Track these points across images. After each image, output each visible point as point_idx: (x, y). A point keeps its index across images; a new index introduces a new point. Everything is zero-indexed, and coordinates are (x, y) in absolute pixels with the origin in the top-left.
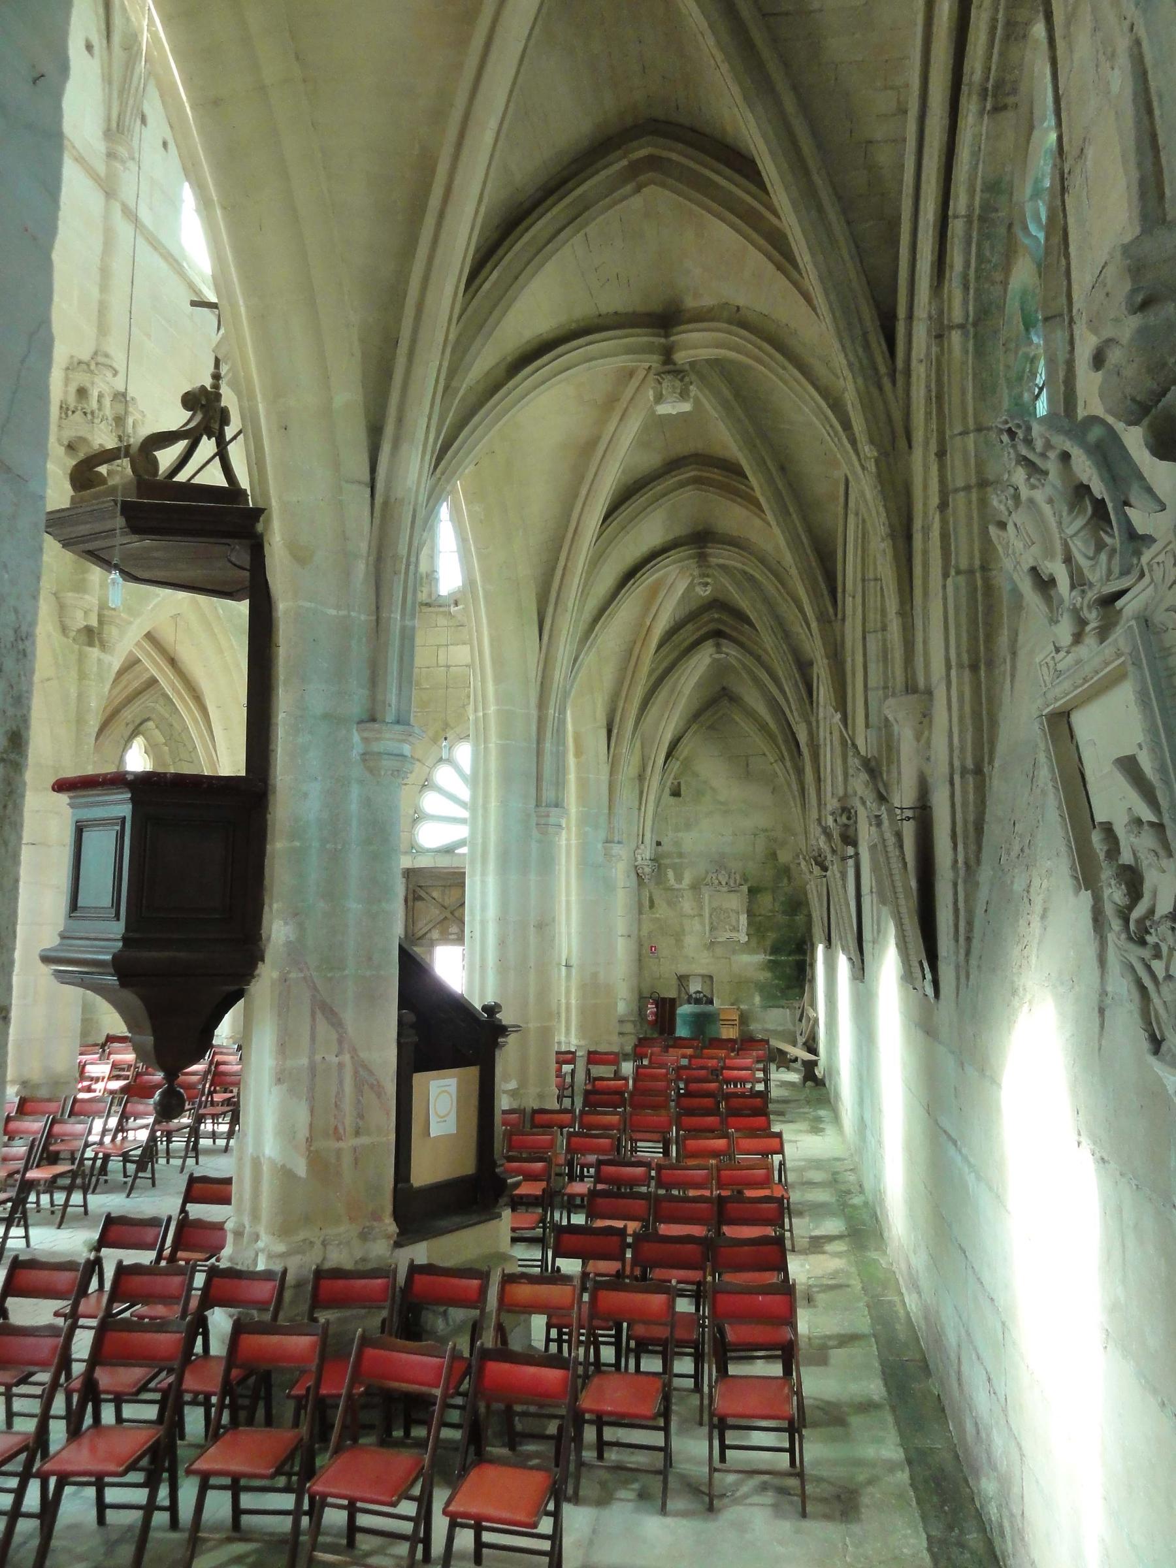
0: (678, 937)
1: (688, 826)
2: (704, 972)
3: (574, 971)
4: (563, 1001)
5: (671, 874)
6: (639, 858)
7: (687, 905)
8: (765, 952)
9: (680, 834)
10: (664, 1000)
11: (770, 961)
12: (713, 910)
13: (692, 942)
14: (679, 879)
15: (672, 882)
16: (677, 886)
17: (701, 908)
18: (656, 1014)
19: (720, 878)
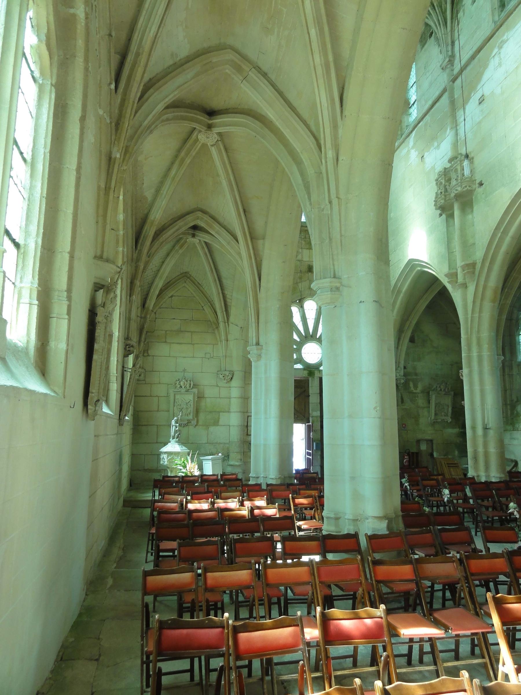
0: (416, 418)
1: (419, 359)
2: (430, 438)
3: (491, 433)
4: (481, 450)
5: (411, 385)
6: (398, 375)
7: (421, 401)
8: (459, 427)
9: (415, 363)
10: (413, 453)
11: (461, 432)
12: (436, 405)
13: (423, 421)
14: (416, 387)
15: (412, 389)
16: (415, 391)
17: (429, 402)
18: (409, 461)
19: (442, 387)
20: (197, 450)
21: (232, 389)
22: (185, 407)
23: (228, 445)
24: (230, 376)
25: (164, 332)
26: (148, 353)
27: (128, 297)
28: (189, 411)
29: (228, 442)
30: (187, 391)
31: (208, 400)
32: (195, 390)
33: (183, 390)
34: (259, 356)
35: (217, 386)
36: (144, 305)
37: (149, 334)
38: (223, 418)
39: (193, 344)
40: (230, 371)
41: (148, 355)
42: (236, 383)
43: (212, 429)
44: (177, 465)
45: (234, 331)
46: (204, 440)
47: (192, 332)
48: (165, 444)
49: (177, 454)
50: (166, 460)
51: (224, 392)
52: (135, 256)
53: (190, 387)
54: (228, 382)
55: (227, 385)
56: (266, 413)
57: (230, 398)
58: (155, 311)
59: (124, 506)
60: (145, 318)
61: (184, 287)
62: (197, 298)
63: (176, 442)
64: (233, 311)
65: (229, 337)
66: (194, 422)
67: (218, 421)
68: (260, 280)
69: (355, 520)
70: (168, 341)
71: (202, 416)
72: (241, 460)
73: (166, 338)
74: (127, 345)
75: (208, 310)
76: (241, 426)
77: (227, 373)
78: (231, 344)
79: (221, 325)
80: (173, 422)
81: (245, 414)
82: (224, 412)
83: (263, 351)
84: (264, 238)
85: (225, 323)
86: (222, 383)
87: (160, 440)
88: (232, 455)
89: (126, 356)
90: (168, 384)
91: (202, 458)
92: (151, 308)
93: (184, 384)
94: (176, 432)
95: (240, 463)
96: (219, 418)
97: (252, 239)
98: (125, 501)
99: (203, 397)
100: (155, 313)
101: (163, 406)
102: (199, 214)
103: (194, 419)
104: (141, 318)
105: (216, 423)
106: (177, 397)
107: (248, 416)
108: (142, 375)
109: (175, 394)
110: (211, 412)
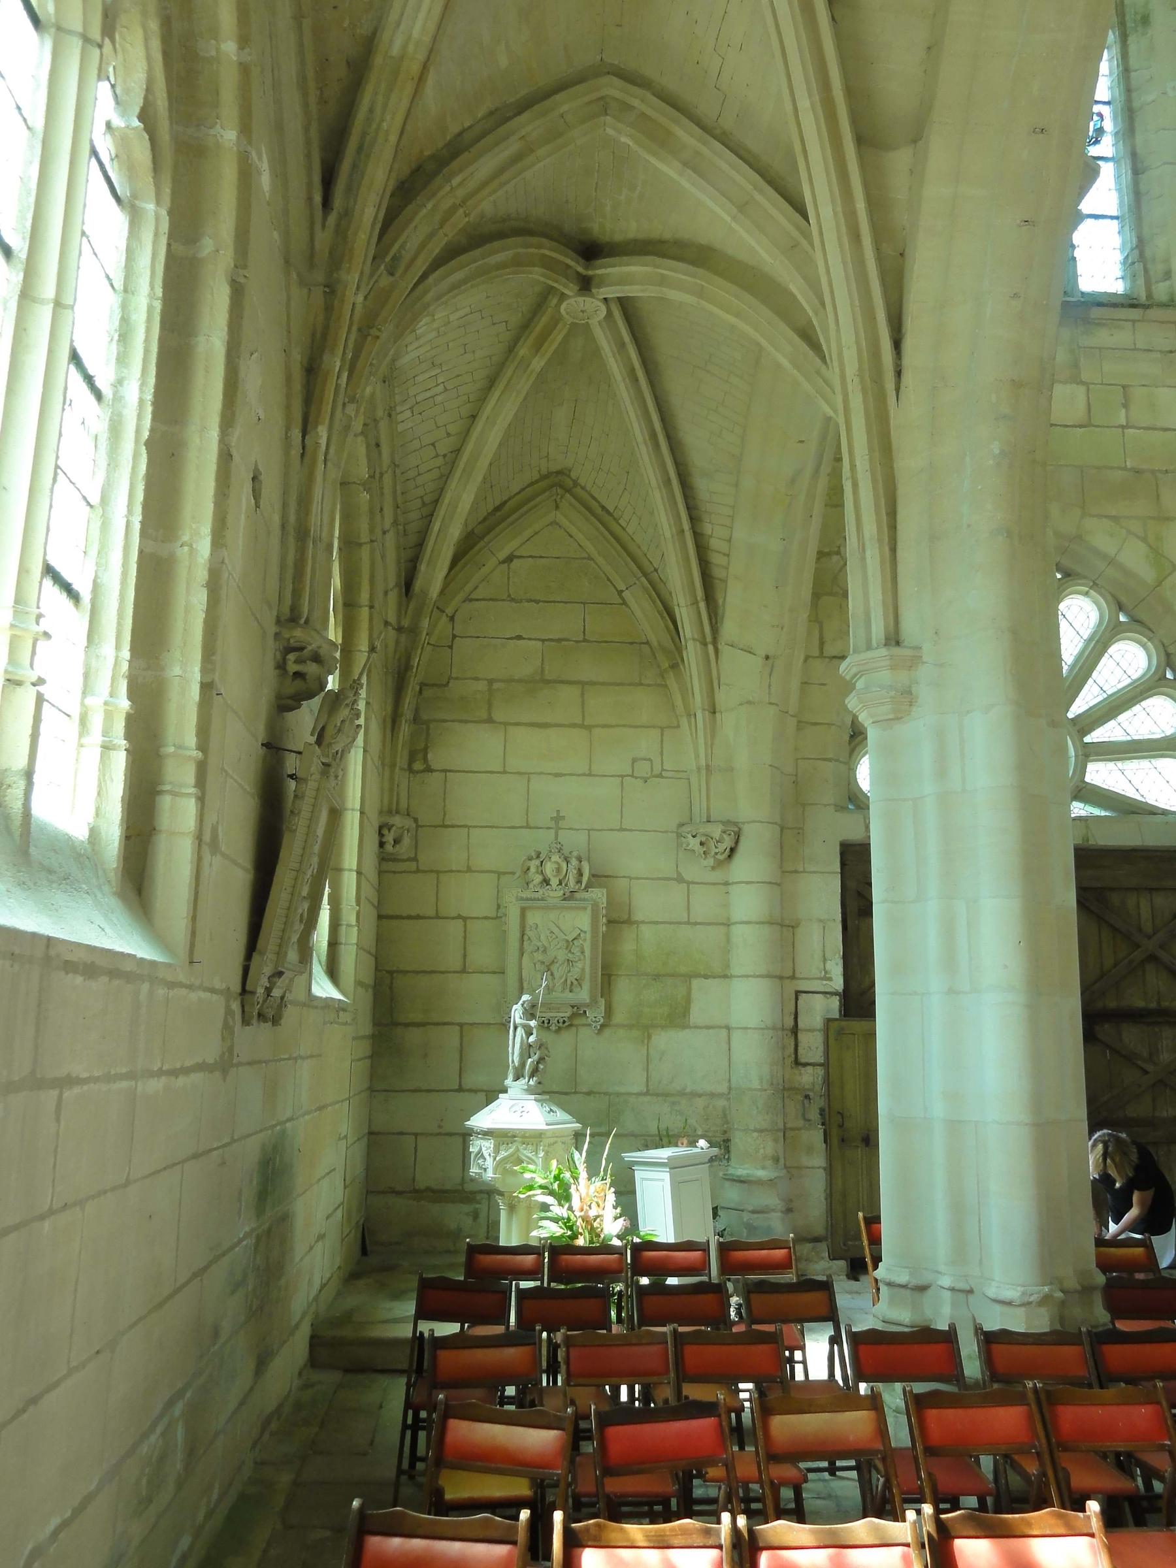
20: (609, 1125)
21: (734, 889)
22: (561, 955)
23: (721, 1103)
24: (728, 843)
25: (482, 686)
26: (425, 759)
27: (296, 433)
28: (576, 972)
29: (723, 1088)
30: (570, 896)
31: (646, 931)
32: (598, 895)
33: (554, 894)
34: (904, 700)
35: (680, 879)
36: (407, 586)
37: (428, 693)
38: (706, 1000)
39: (589, 728)
40: (728, 823)
41: (429, 770)
42: (751, 866)
43: (663, 1040)
44: (531, 1188)
45: (741, 675)
46: (635, 1083)
47: (583, 684)
48: (491, 1095)
49: (533, 1138)
50: (489, 1163)
51: (704, 904)
52: (323, 239)
53: (579, 882)
54: (718, 865)
55: (717, 876)
56: (950, 962)
57: (728, 924)
58: (449, 611)
59: (314, 1361)
60: (413, 631)
61: (554, 523)
62: (600, 560)
63: (530, 1091)
64: (733, 599)
65: (721, 696)
66: (596, 1015)
67: (686, 1012)
68: (897, 344)
70: (498, 715)
71: (625, 993)
72: (776, 1160)
73: (490, 706)
74: (289, 650)
75: (641, 607)
76: (774, 1028)
77: (716, 831)
78: (728, 722)
79: (692, 653)
80: (517, 1013)
81: (787, 982)
82: (706, 977)
83: (924, 673)
84: (917, 137)
85: (705, 644)
86: (697, 870)
87: (470, 1081)
88: (740, 1141)
89: (286, 704)
90: (500, 874)
91: (629, 1156)
92: (434, 592)
93: (558, 870)
94: (527, 1050)
95: (776, 1174)
96: (688, 999)
97: (860, 140)
98: (315, 1341)
99: (629, 922)
100: (452, 619)
101: (481, 955)
102: (613, 88)
103: (594, 1002)
104: (399, 629)
105: (678, 1017)
106: (533, 918)
107: (798, 993)
108: (407, 841)
109: (523, 911)
110: (657, 977)
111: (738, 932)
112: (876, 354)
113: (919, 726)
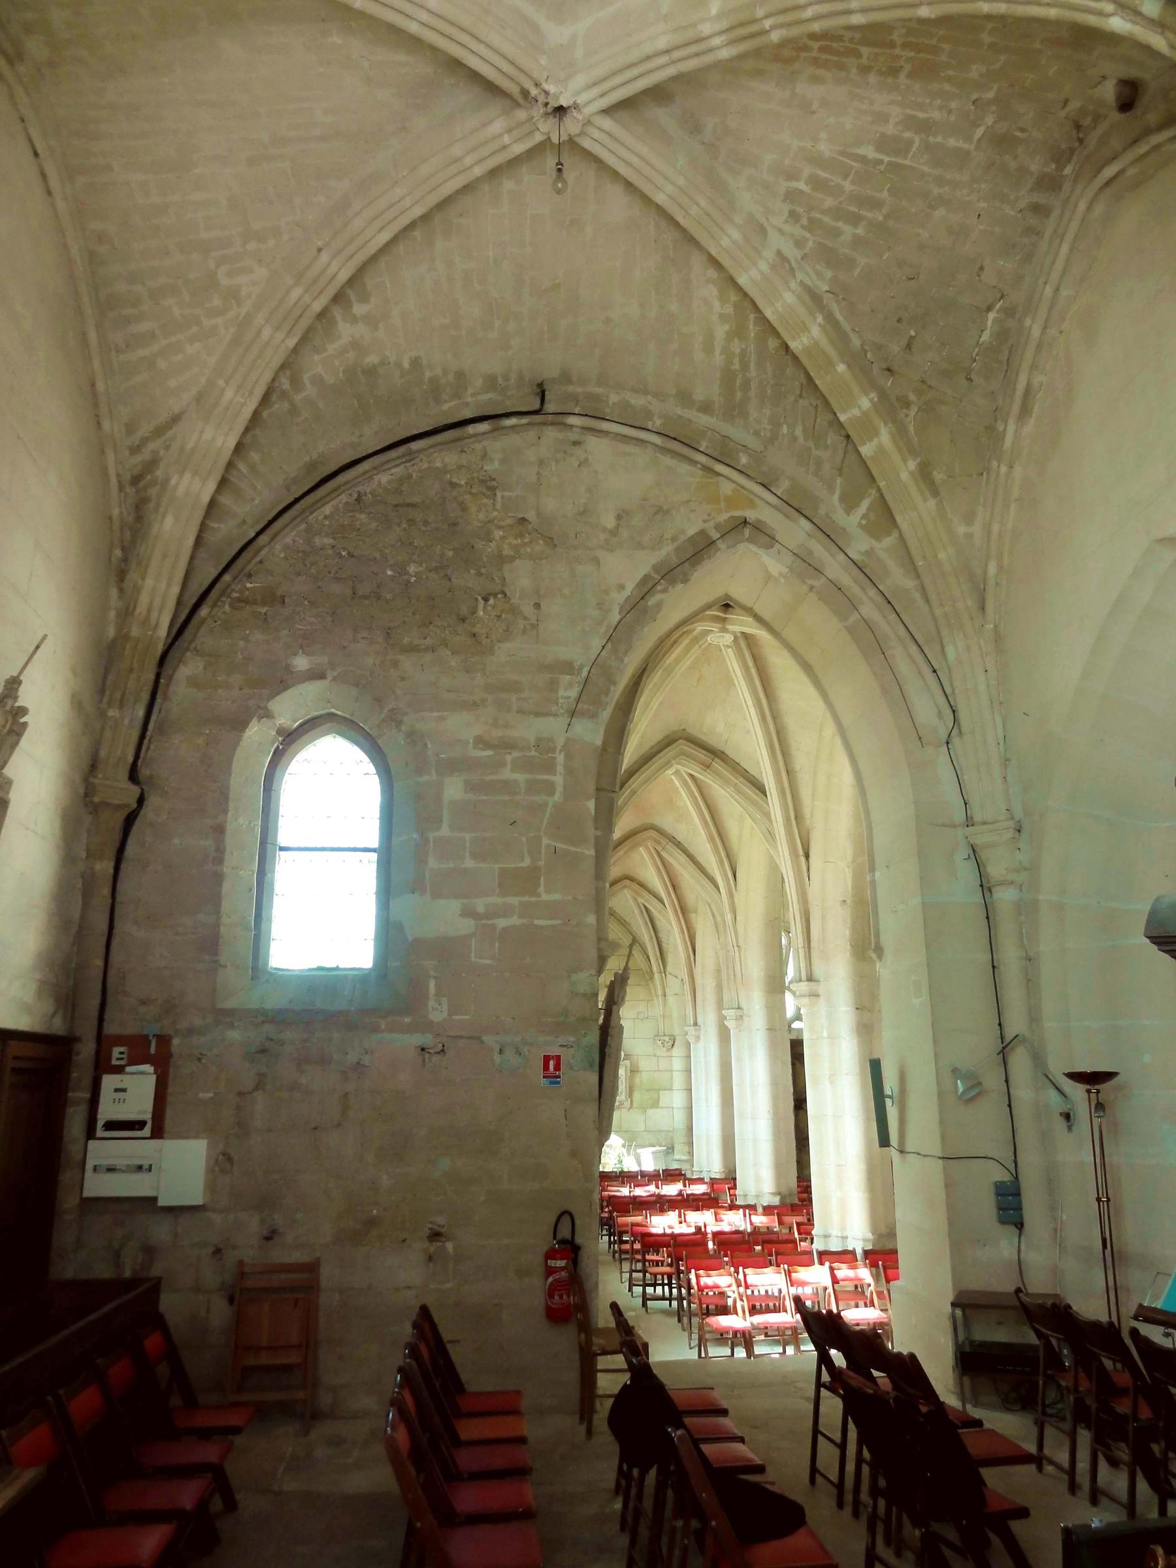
31: (644, 1075)
34: (698, 1038)
38: (664, 1098)
42: (678, 1051)
43: (651, 1112)
45: (673, 985)
46: (642, 1127)
51: (663, 1064)
54: (668, 1050)
57: (671, 1071)
64: (670, 960)
66: (627, 1104)
69: (758, 1196)
71: (637, 1095)
77: (667, 1039)
78: (671, 1000)
79: (656, 976)
86: (662, 1052)
88: (678, 1147)
97: (683, 914)
102: (627, 882)
105: (655, 1104)
110: (648, 1090)
111: (675, 1074)
112: (689, 957)
113: (701, 1044)
